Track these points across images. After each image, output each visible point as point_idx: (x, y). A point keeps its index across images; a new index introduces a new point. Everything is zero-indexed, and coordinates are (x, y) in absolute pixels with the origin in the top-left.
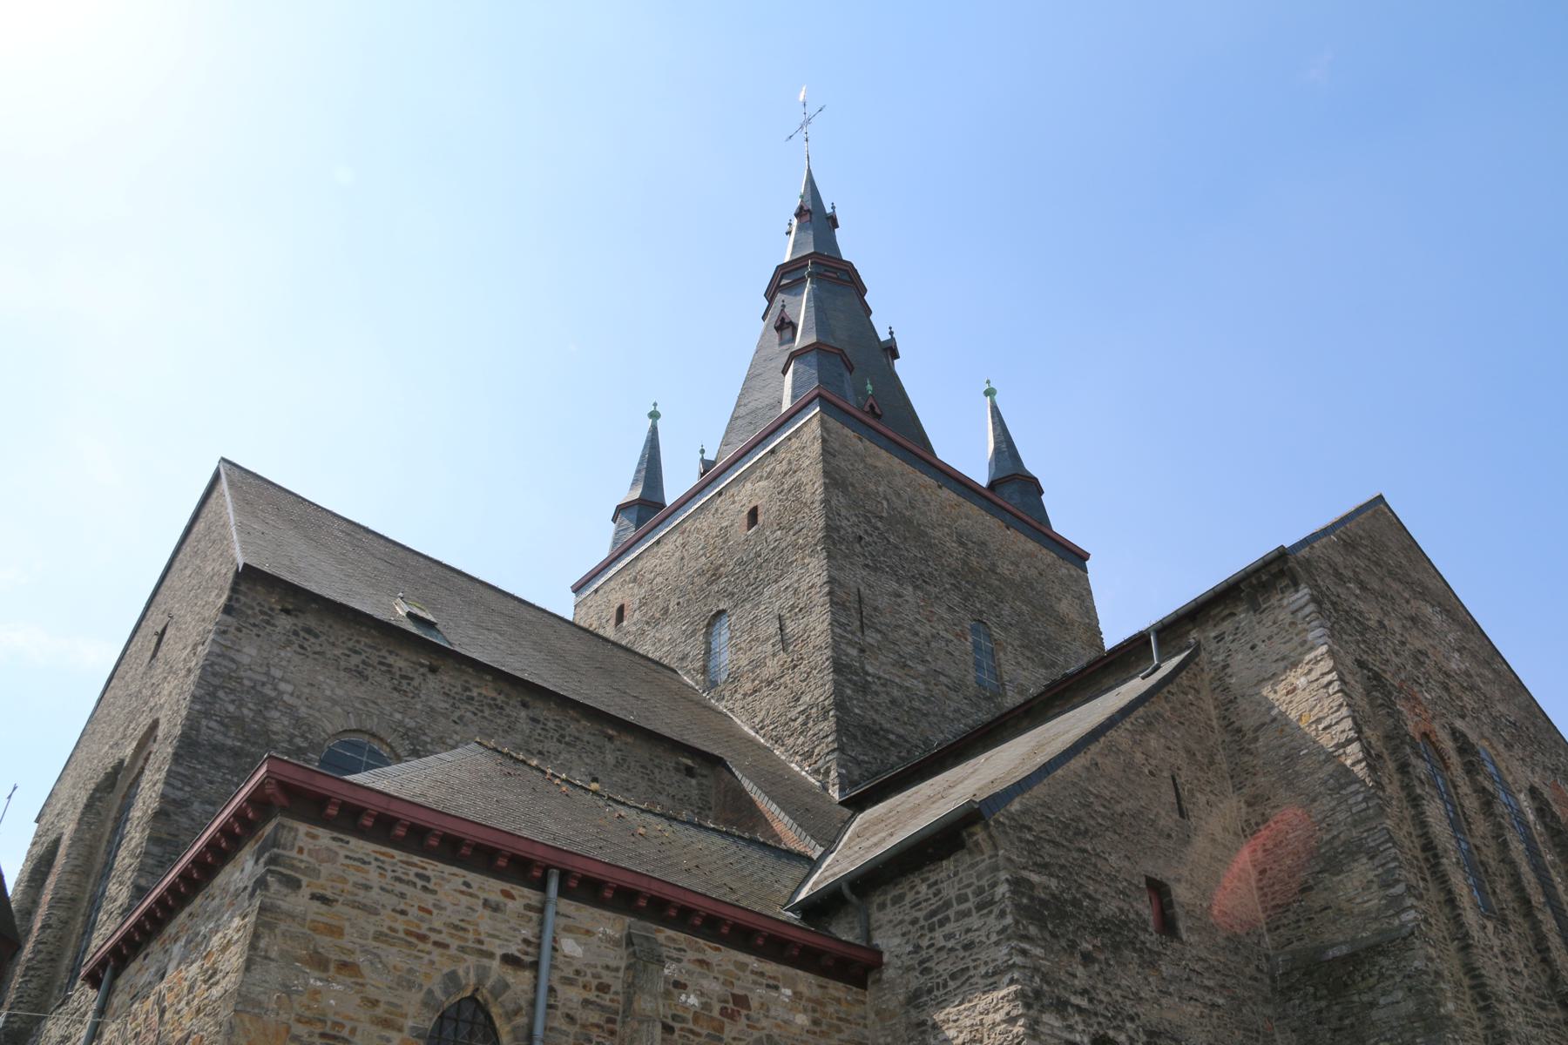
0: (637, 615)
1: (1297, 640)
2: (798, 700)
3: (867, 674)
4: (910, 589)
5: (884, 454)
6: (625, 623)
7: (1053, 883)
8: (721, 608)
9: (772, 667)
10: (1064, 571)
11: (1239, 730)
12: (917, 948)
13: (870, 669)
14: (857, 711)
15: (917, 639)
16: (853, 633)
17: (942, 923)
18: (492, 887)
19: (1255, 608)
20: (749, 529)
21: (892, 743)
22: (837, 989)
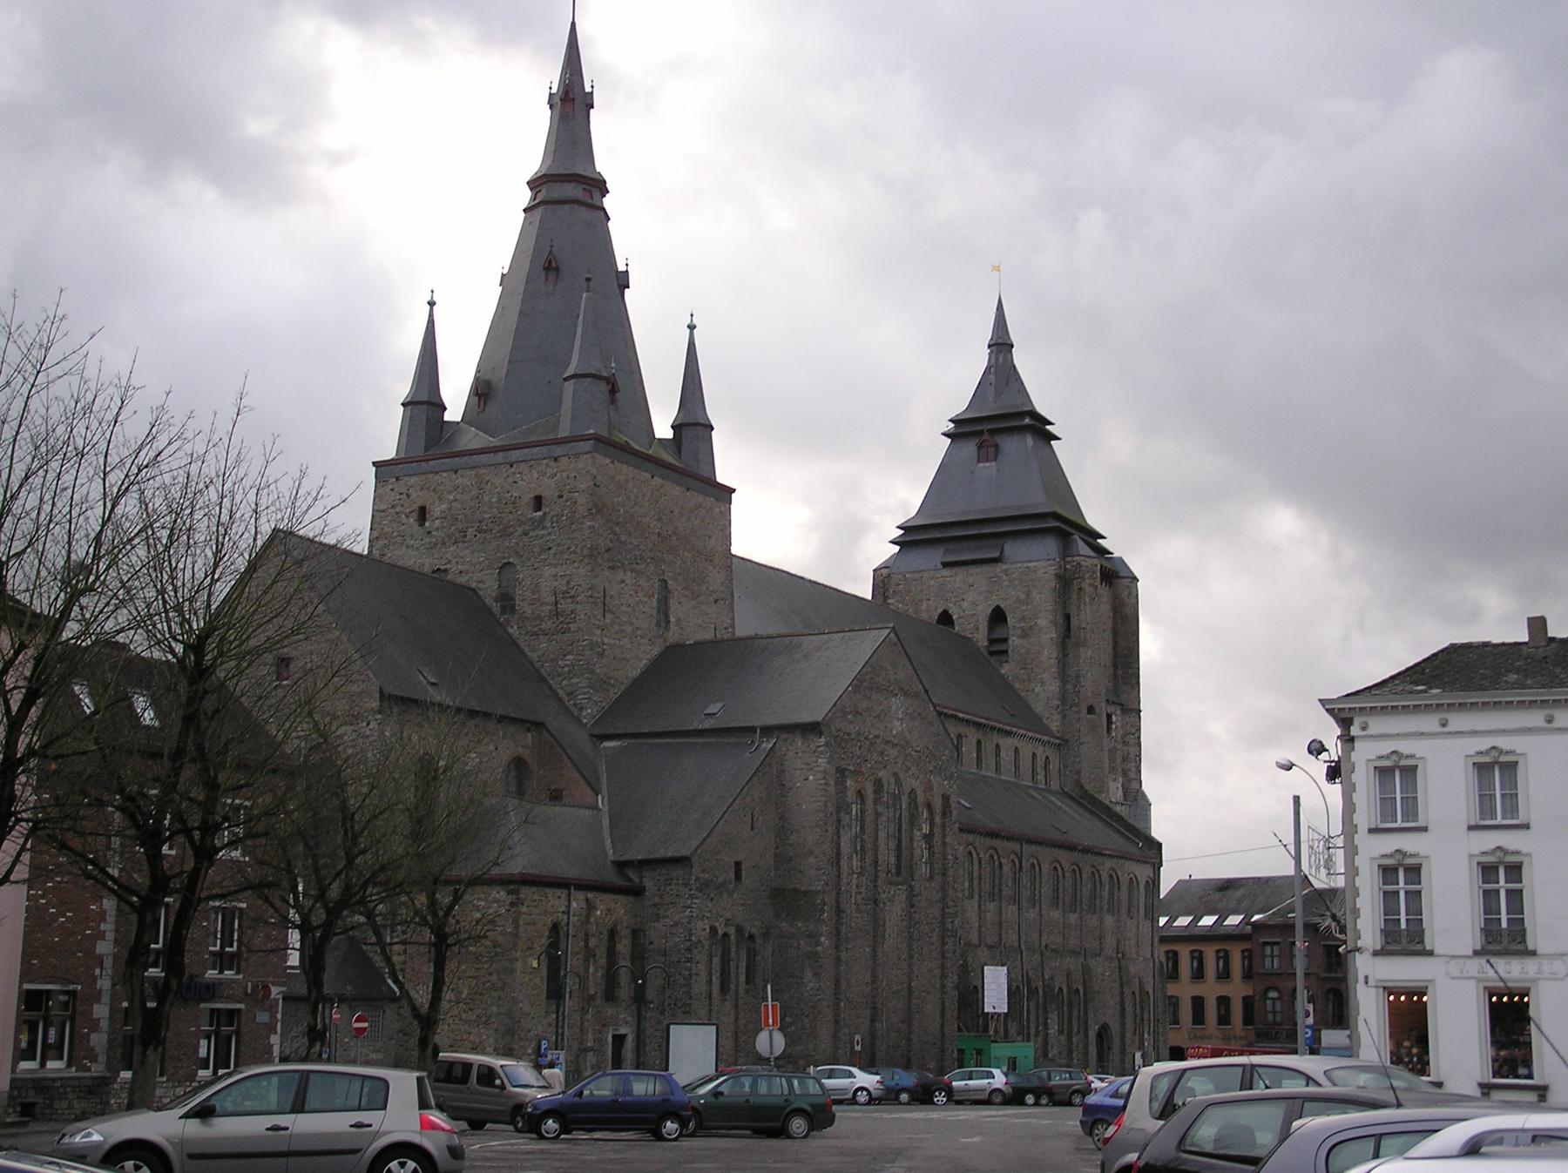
0: (437, 522)
1: (814, 759)
2: (565, 655)
3: (604, 644)
4: (629, 573)
5: (625, 467)
6: (427, 524)
7: (707, 876)
8: (511, 560)
9: (548, 625)
10: (718, 510)
11: (783, 785)
12: (659, 890)
13: (606, 640)
14: (598, 671)
15: (630, 609)
16: (599, 620)
17: (670, 884)
18: (558, 892)
19: (803, 736)
20: (536, 511)
21: (613, 686)
22: (631, 899)
